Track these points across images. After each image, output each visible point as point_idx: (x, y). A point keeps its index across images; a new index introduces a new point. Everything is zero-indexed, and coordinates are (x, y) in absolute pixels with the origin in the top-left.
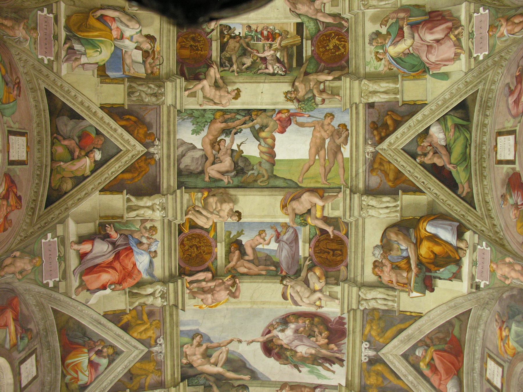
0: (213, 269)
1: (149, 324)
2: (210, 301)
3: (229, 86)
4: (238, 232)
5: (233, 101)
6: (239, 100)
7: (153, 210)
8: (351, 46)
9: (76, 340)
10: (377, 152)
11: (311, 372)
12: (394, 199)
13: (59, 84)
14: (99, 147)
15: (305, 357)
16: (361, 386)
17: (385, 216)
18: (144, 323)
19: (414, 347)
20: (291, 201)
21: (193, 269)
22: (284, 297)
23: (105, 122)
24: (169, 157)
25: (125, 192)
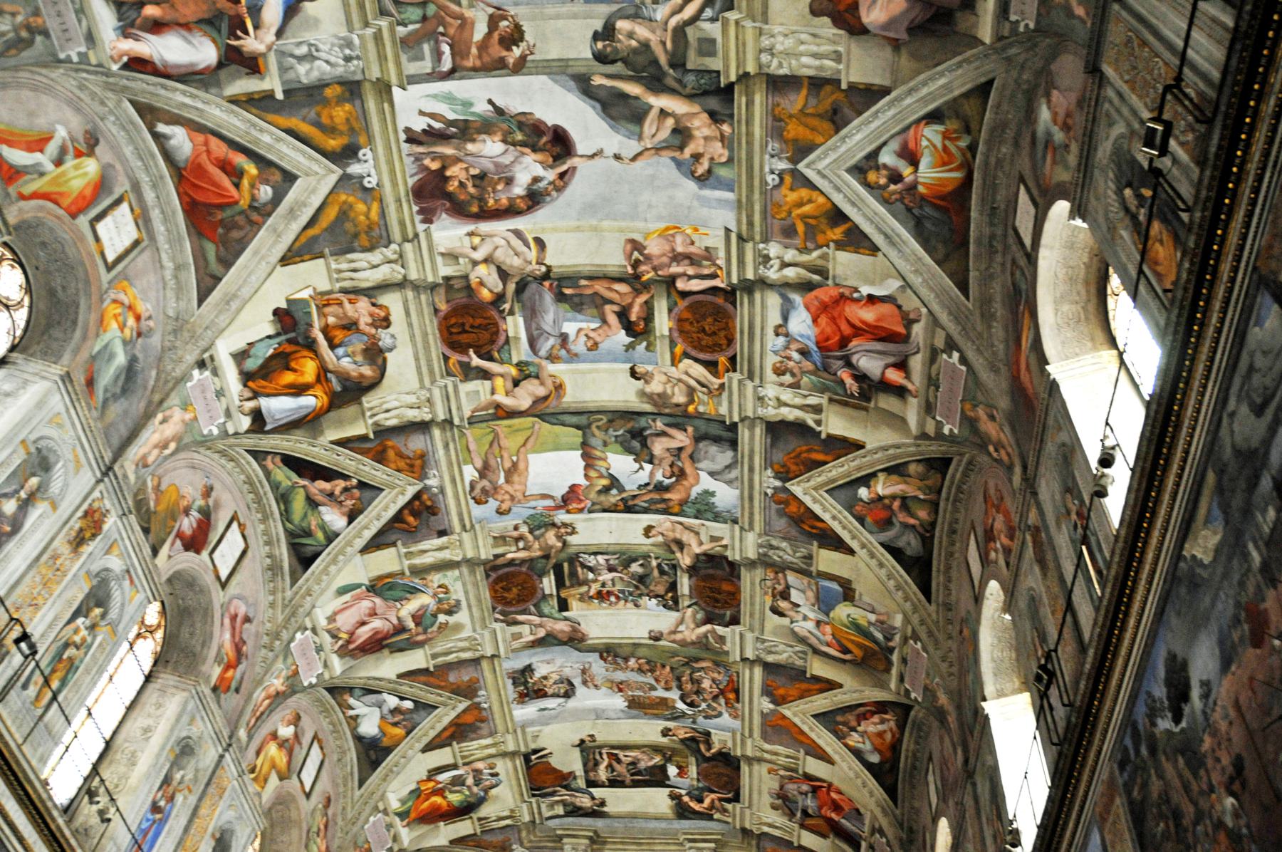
0: (674, 294)
2: (679, 239)
6: (645, 524)
7: (778, 399)
8: (486, 594)
10: (421, 480)
11: (467, 104)
13: (908, 604)
16: (360, 96)
17: (388, 399)
18: (803, 217)
21: (709, 298)
22: (540, 243)
23: (850, 532)
24: (751, 470)
25: (823, 436)
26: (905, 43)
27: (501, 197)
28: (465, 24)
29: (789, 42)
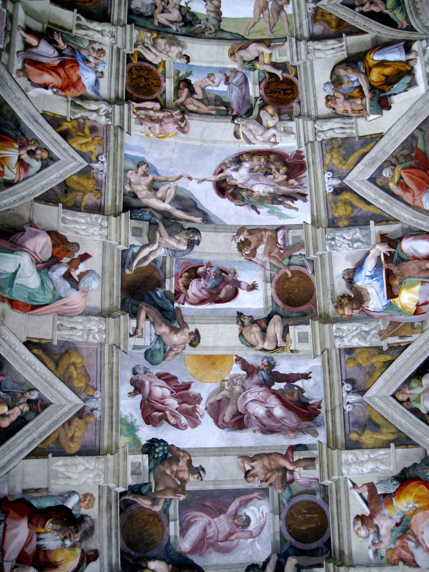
0: (162, 101)
1: (91, 138)
2: (157, 131)
4: (187, 73)
7: (103, 35)
9: (8, 131)
11: (271, 212)
12: (339, 41)
15: (263, 197)
16: (329, 220)
17: (332, 56)
18: (85, 136)
19: (380, 169)
20: (238, 50)
21: (141, 97)
22: (236, 135)
25: (76, 10)
28: (269, 254)
29: (91, 231)
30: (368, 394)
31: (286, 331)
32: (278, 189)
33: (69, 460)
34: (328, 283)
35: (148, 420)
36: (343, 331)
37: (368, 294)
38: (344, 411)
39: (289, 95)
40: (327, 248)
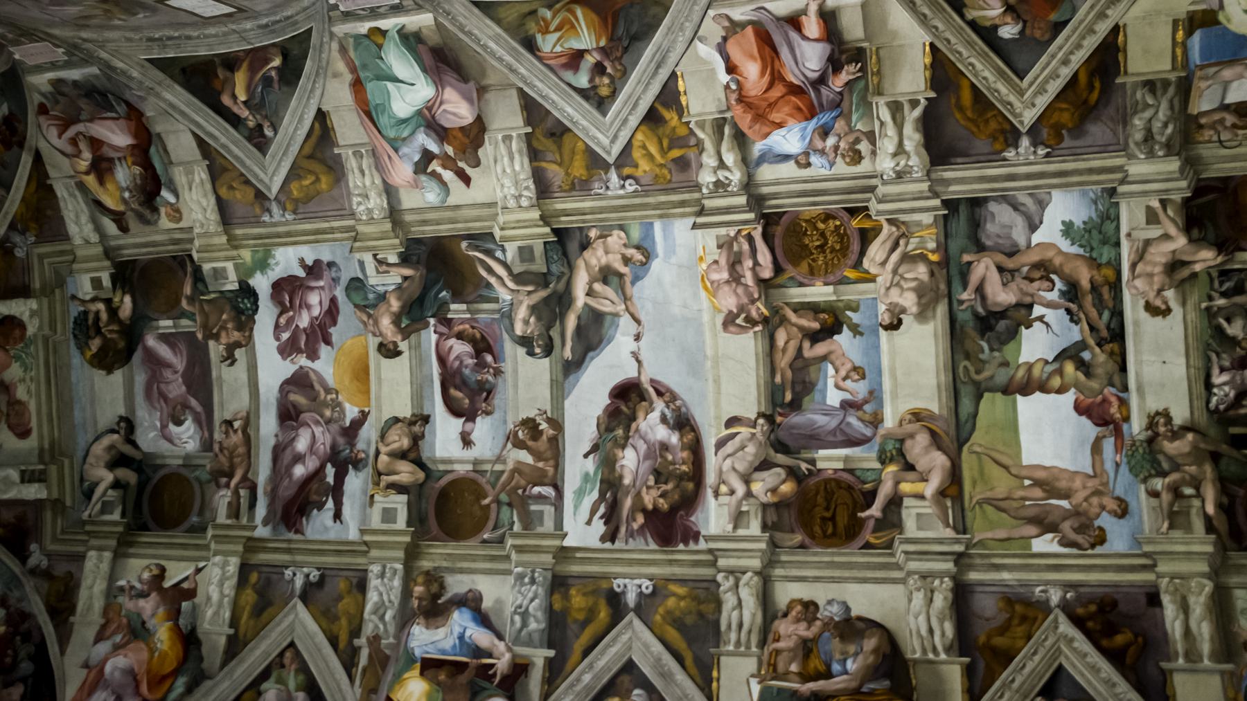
0: (780, 280)
1: (663, 162)
2: (715, 276)
3: (1177, 292)
4: (857, 326)
5: (1142, 303)
6: (1144, 315)
7: (895, 155)
14: (1028, 32)
15: (614, 465)
18: (663, 152)
21: (778, 242)
22: (732, 422)
23: (1084, 38)
25: (932, 95)
26: (477, 83)
27: (680, 458)
28: (518, 469)
29: (507, 182)
30: (300, 606)
31: (400, 488)
32: (628, 493)
33: (208, 186)
34: (465, 565)
35: (278, 286)
36: (391, 580)
37: (437, 628)
38: (287, 567)
39: (821, 528)
40: (519, 569)
